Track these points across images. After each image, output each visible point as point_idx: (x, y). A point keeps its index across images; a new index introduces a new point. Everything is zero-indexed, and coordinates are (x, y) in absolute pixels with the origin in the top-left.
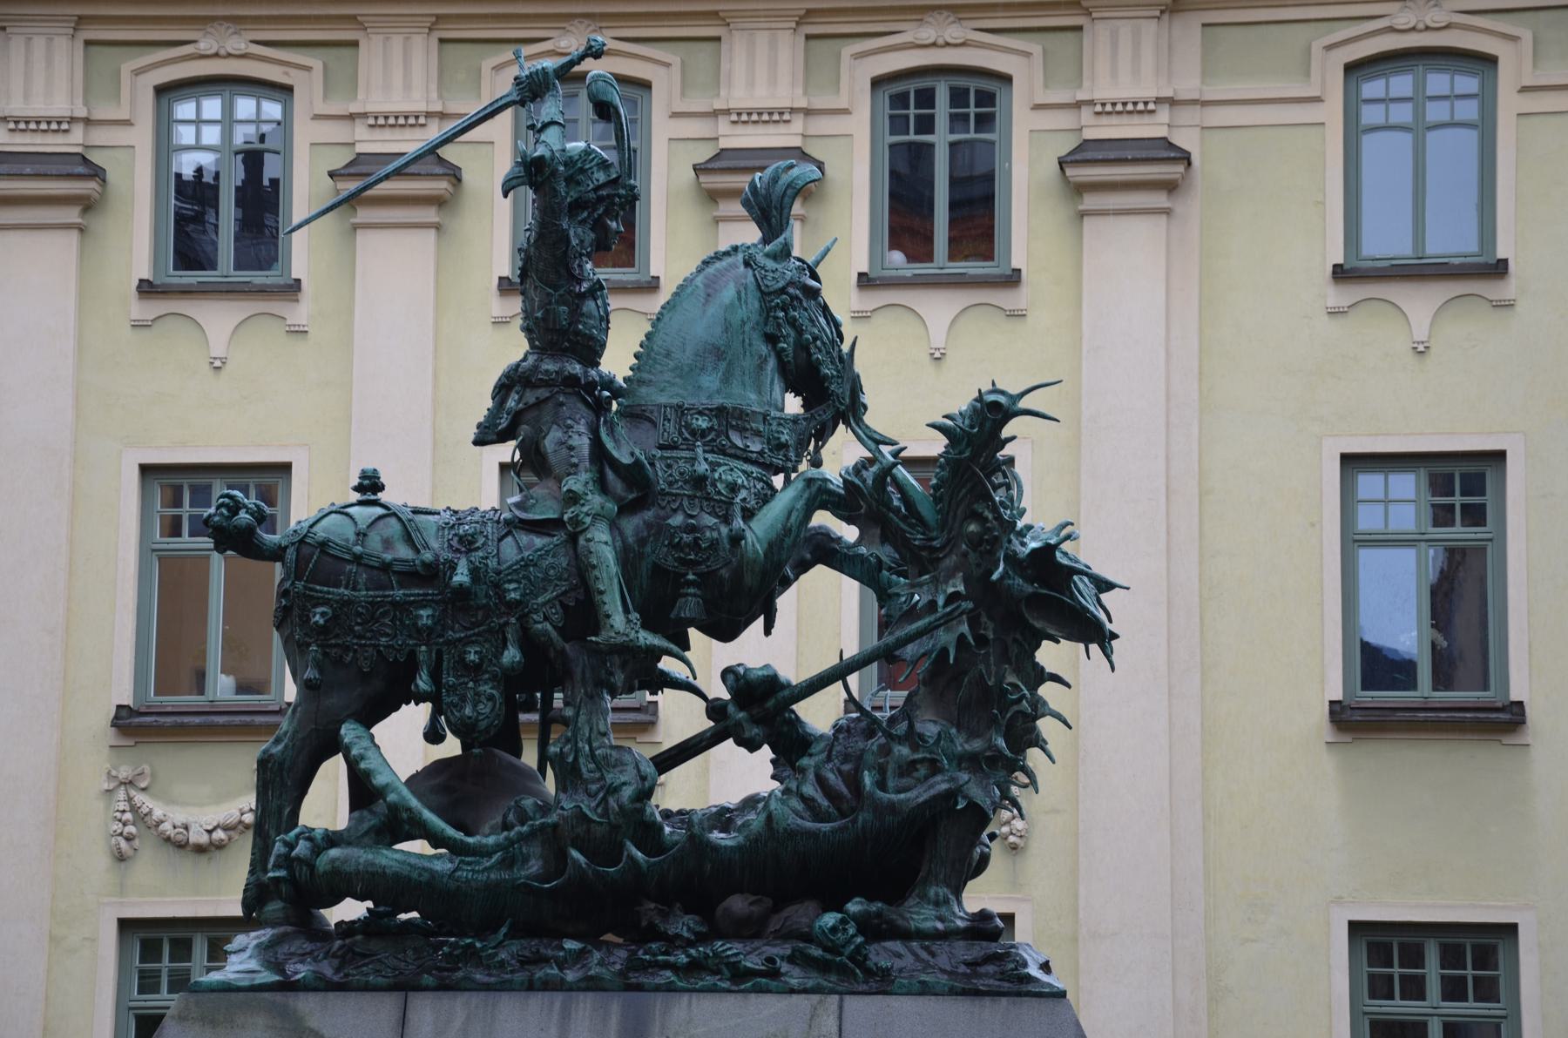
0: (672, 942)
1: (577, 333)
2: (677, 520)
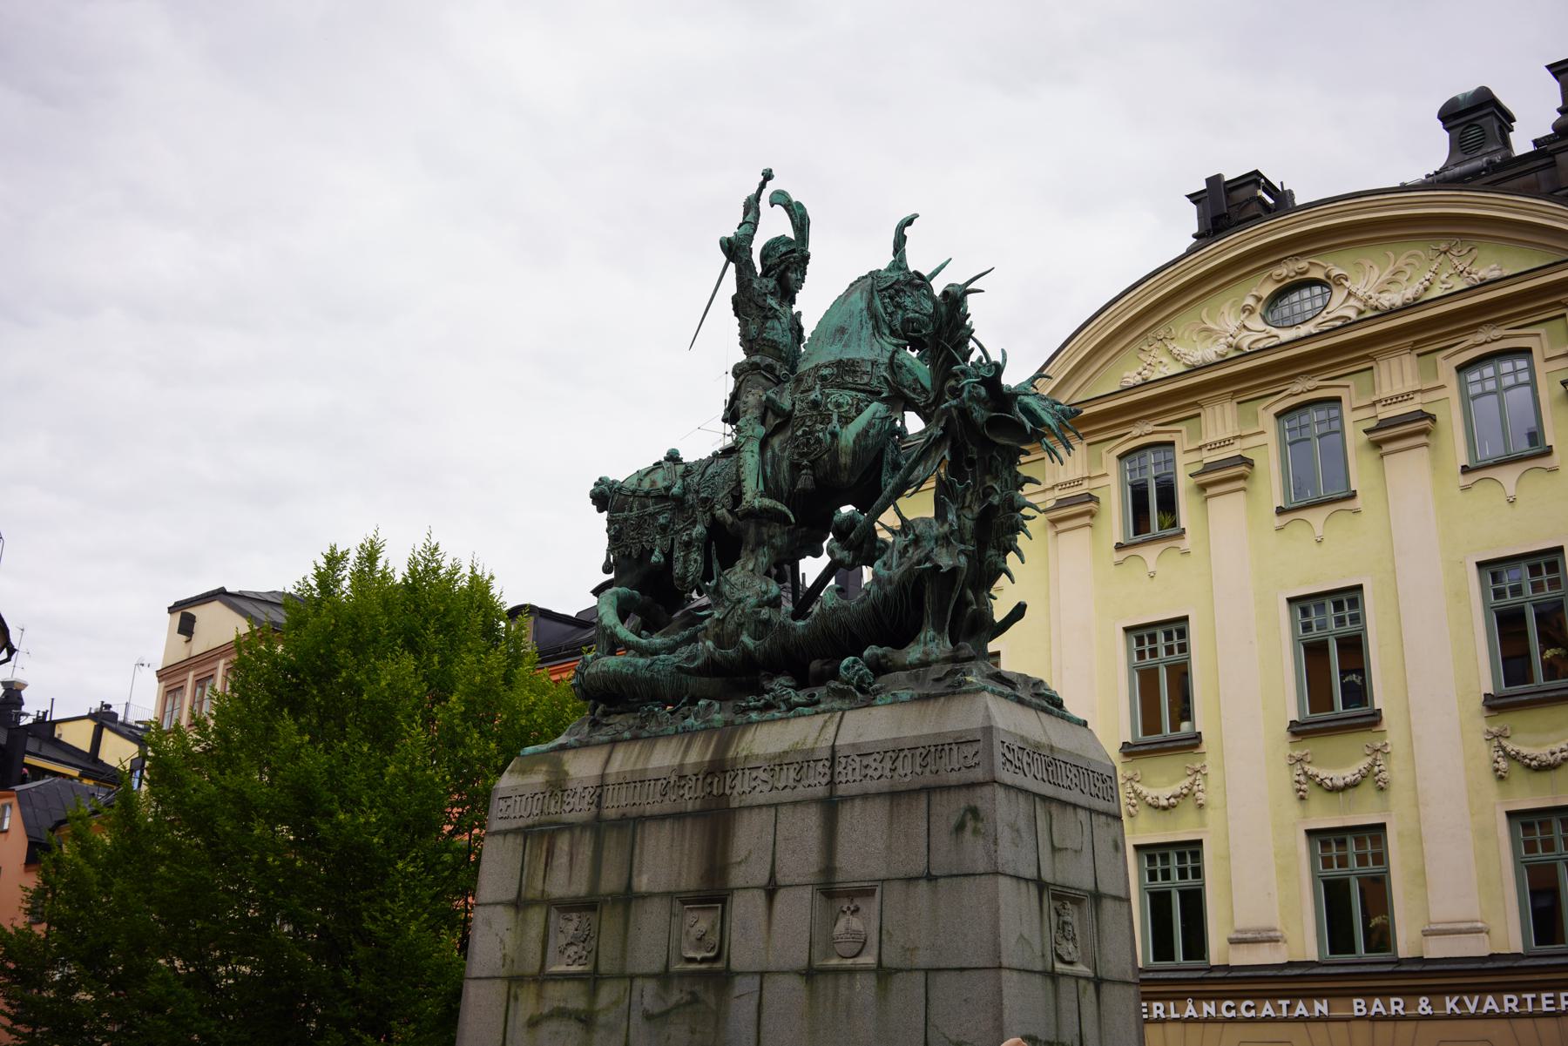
1: (764, 339)
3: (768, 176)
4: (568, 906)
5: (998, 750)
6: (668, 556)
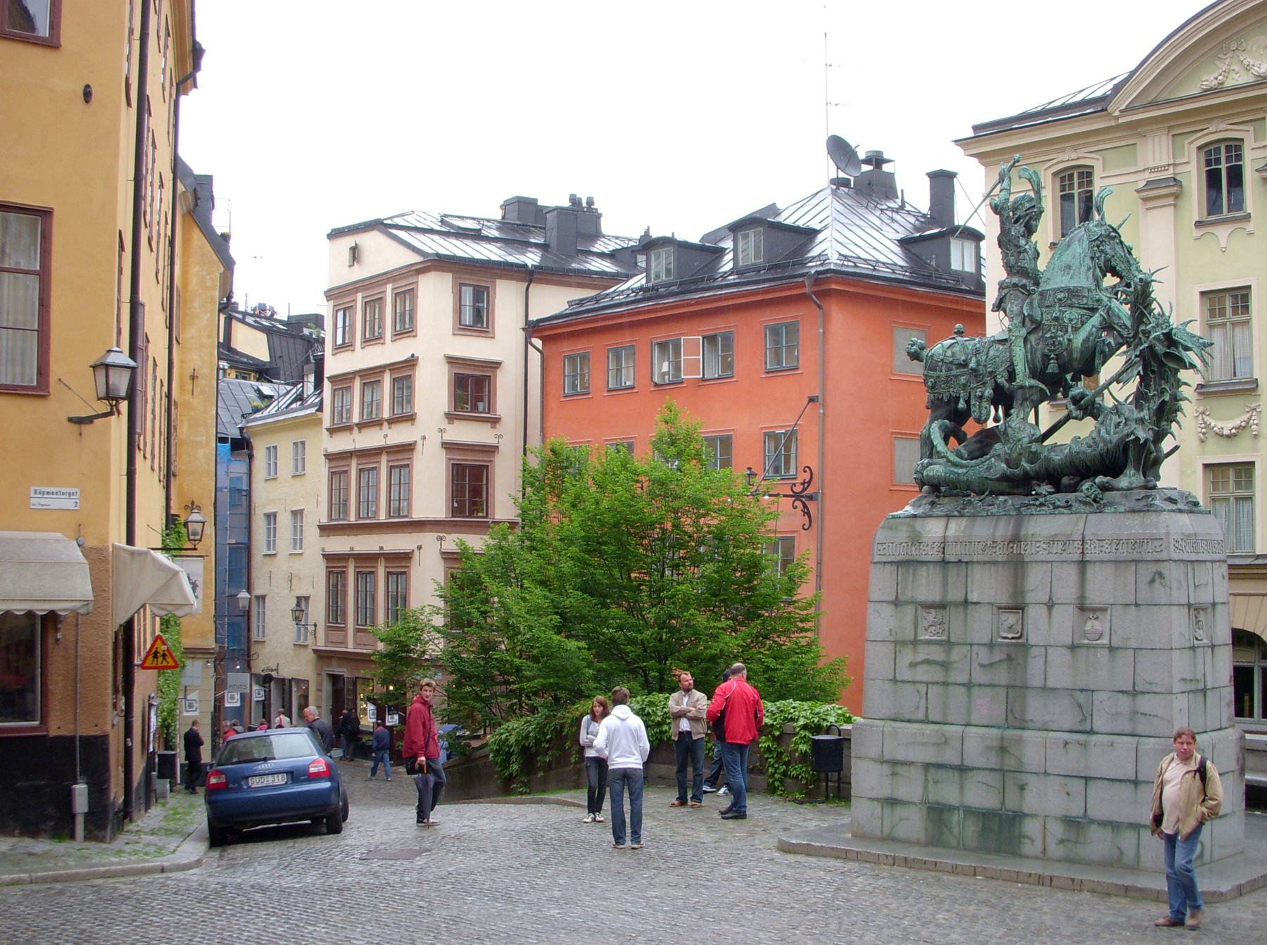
2: (1048, 335)
5: (1172, 542)
6: (968, 402)
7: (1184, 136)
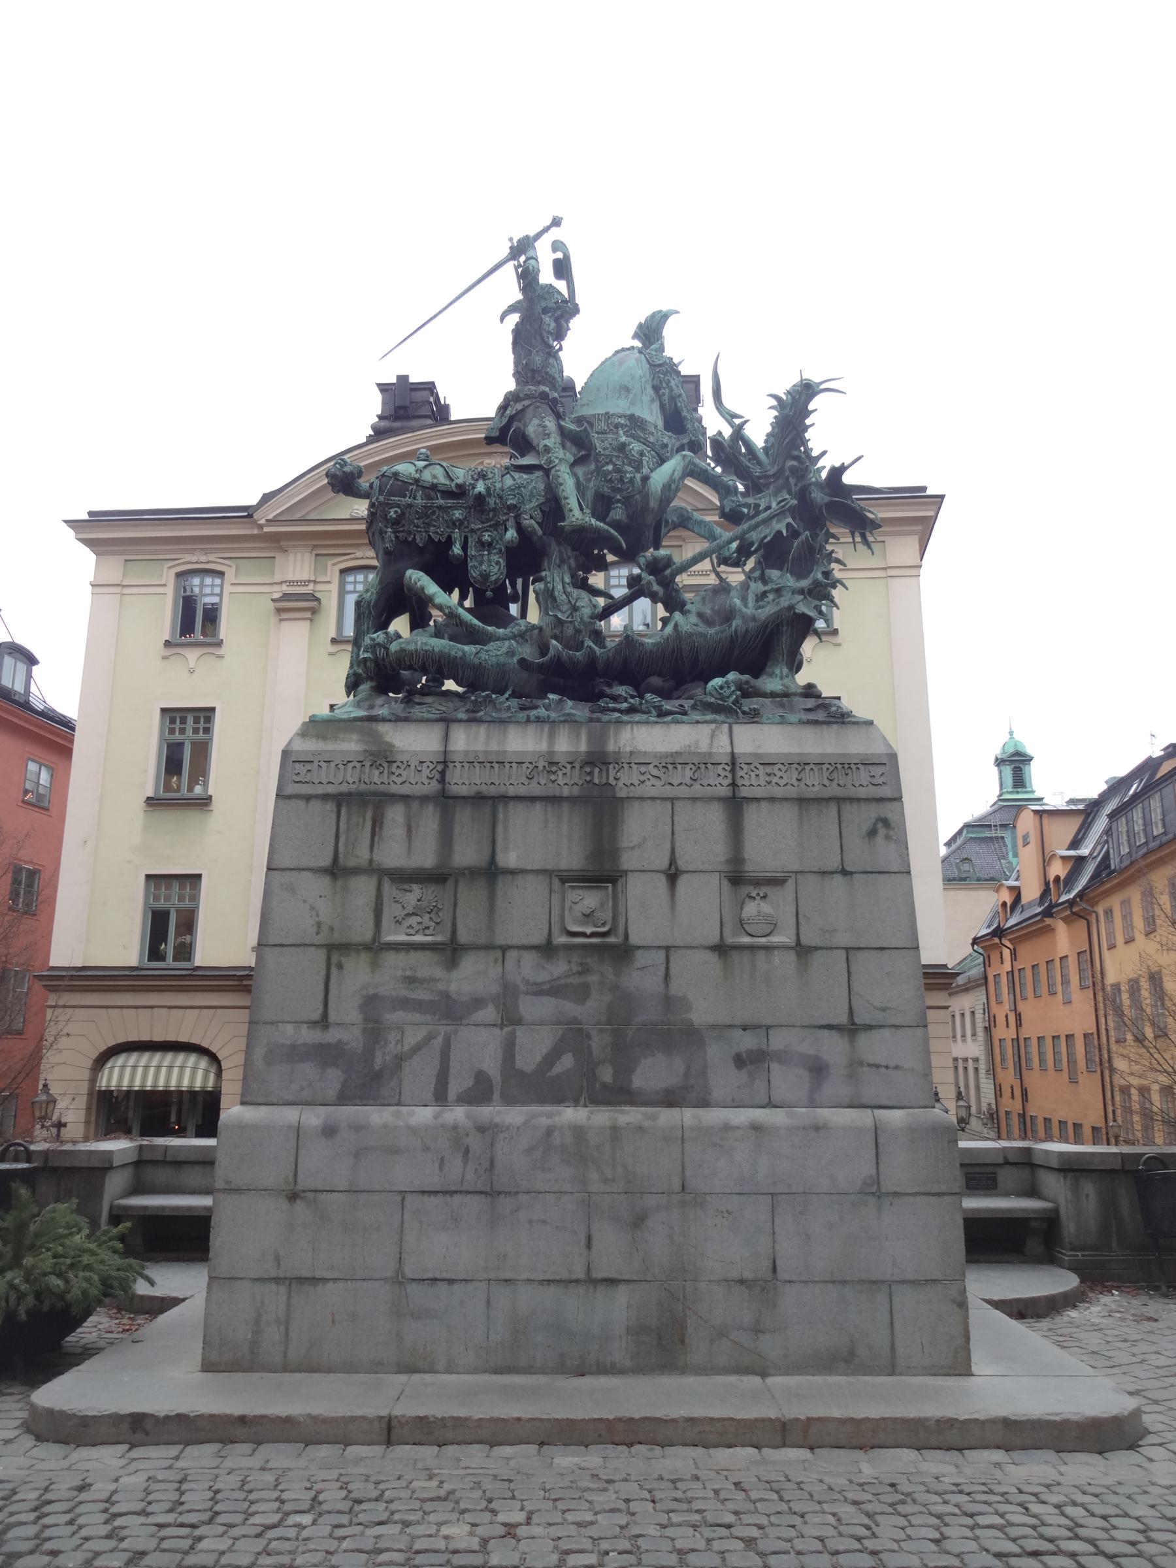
0: (615, 698)
1: (547, 373)
2: (610, 467)
3: (556, 222)
4: (404, 877)
7: (326, 557)
